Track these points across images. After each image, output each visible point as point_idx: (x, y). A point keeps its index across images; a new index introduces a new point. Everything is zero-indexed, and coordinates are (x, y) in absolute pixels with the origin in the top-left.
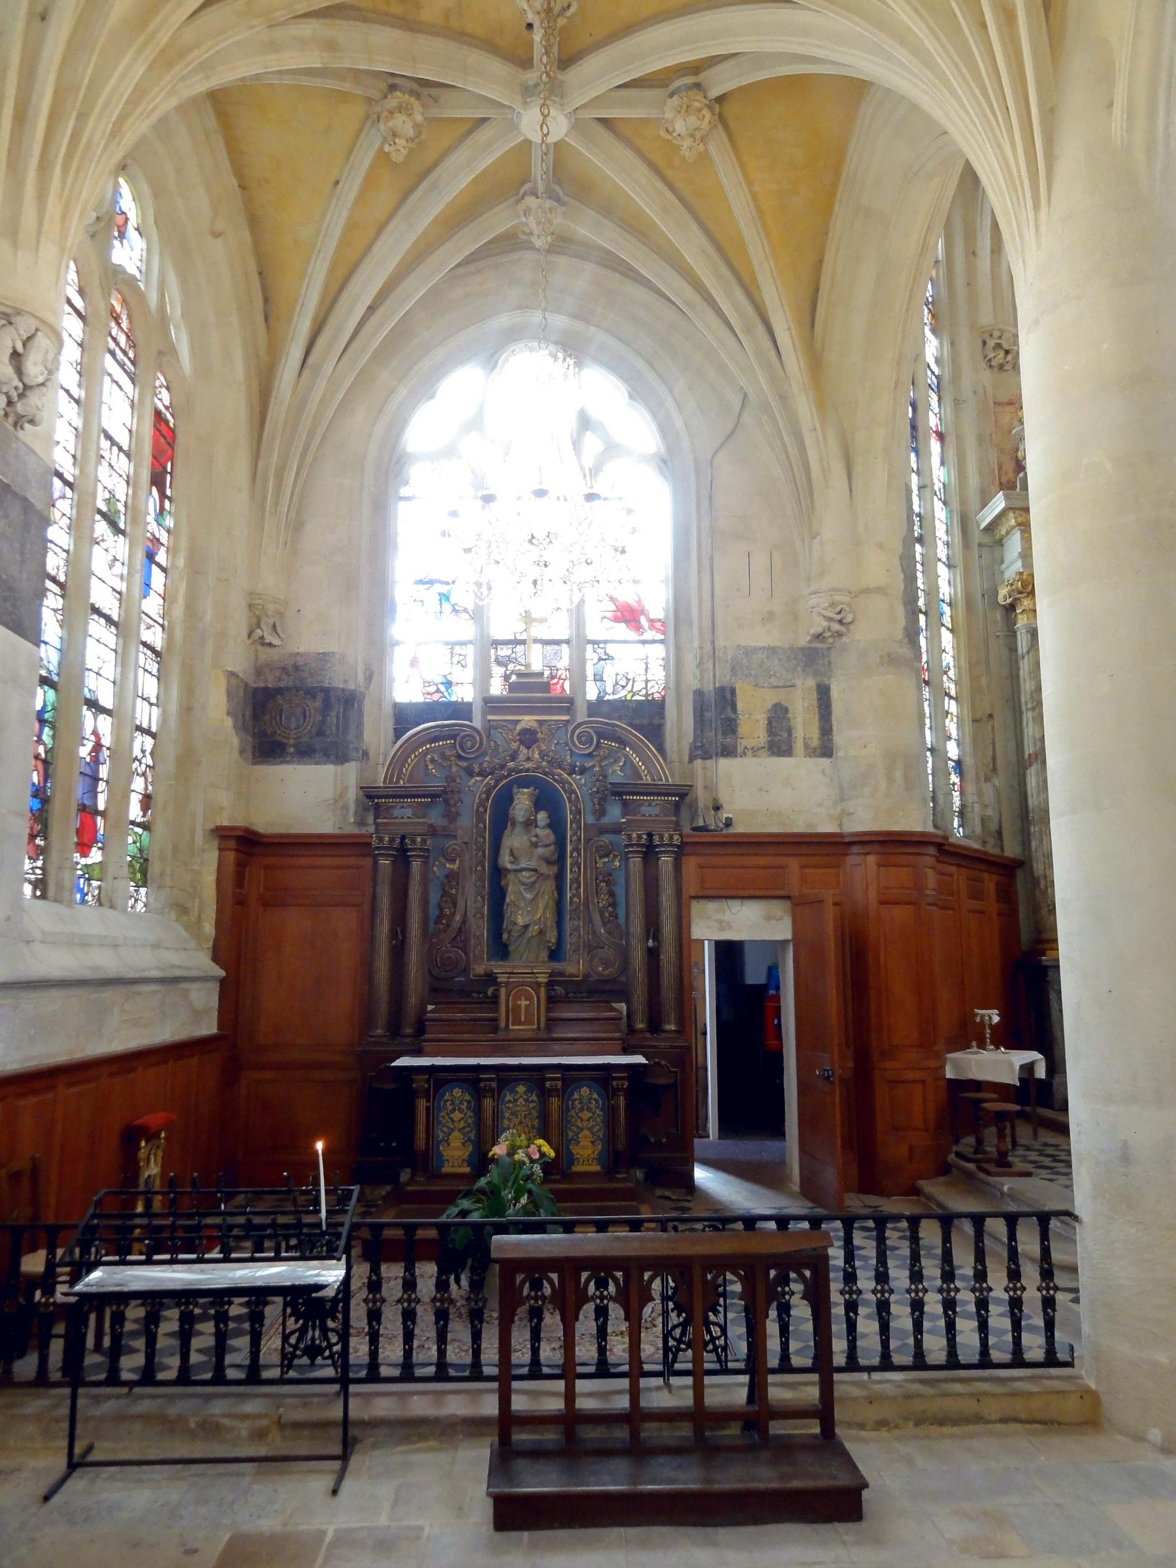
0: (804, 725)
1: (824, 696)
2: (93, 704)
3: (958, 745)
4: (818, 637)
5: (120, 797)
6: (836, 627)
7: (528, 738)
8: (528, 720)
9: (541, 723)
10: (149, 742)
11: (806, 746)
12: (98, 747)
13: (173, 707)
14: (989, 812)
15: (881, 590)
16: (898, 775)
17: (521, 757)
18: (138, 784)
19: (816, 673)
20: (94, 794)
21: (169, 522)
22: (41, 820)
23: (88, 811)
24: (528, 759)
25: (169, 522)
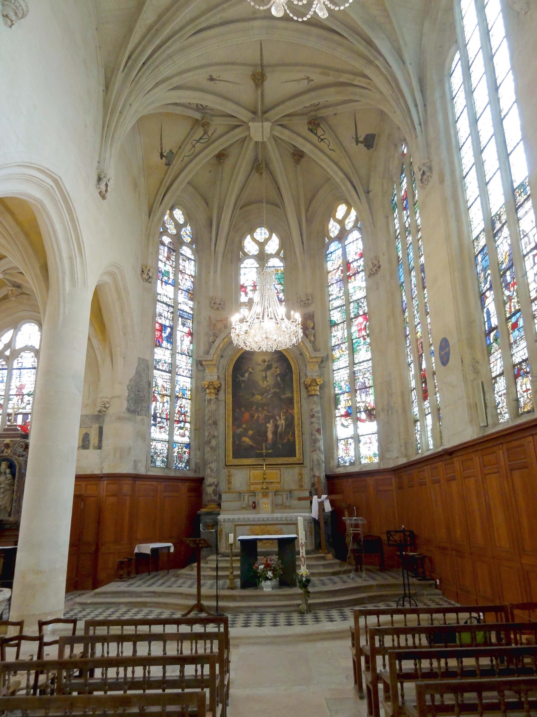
0: (94, 440)
1: (101, 430)
3: (189, 438)
4: (100, 411)
6: (103, 409)
7: (7, 446)
8: (7, 441)
9: (11, 441)
11: (93, 446)
14: (198, 461)
15: (118, 397)
16: (118, 455)
17: (5, 452)
19: (99, 423)
24: (6, 453)
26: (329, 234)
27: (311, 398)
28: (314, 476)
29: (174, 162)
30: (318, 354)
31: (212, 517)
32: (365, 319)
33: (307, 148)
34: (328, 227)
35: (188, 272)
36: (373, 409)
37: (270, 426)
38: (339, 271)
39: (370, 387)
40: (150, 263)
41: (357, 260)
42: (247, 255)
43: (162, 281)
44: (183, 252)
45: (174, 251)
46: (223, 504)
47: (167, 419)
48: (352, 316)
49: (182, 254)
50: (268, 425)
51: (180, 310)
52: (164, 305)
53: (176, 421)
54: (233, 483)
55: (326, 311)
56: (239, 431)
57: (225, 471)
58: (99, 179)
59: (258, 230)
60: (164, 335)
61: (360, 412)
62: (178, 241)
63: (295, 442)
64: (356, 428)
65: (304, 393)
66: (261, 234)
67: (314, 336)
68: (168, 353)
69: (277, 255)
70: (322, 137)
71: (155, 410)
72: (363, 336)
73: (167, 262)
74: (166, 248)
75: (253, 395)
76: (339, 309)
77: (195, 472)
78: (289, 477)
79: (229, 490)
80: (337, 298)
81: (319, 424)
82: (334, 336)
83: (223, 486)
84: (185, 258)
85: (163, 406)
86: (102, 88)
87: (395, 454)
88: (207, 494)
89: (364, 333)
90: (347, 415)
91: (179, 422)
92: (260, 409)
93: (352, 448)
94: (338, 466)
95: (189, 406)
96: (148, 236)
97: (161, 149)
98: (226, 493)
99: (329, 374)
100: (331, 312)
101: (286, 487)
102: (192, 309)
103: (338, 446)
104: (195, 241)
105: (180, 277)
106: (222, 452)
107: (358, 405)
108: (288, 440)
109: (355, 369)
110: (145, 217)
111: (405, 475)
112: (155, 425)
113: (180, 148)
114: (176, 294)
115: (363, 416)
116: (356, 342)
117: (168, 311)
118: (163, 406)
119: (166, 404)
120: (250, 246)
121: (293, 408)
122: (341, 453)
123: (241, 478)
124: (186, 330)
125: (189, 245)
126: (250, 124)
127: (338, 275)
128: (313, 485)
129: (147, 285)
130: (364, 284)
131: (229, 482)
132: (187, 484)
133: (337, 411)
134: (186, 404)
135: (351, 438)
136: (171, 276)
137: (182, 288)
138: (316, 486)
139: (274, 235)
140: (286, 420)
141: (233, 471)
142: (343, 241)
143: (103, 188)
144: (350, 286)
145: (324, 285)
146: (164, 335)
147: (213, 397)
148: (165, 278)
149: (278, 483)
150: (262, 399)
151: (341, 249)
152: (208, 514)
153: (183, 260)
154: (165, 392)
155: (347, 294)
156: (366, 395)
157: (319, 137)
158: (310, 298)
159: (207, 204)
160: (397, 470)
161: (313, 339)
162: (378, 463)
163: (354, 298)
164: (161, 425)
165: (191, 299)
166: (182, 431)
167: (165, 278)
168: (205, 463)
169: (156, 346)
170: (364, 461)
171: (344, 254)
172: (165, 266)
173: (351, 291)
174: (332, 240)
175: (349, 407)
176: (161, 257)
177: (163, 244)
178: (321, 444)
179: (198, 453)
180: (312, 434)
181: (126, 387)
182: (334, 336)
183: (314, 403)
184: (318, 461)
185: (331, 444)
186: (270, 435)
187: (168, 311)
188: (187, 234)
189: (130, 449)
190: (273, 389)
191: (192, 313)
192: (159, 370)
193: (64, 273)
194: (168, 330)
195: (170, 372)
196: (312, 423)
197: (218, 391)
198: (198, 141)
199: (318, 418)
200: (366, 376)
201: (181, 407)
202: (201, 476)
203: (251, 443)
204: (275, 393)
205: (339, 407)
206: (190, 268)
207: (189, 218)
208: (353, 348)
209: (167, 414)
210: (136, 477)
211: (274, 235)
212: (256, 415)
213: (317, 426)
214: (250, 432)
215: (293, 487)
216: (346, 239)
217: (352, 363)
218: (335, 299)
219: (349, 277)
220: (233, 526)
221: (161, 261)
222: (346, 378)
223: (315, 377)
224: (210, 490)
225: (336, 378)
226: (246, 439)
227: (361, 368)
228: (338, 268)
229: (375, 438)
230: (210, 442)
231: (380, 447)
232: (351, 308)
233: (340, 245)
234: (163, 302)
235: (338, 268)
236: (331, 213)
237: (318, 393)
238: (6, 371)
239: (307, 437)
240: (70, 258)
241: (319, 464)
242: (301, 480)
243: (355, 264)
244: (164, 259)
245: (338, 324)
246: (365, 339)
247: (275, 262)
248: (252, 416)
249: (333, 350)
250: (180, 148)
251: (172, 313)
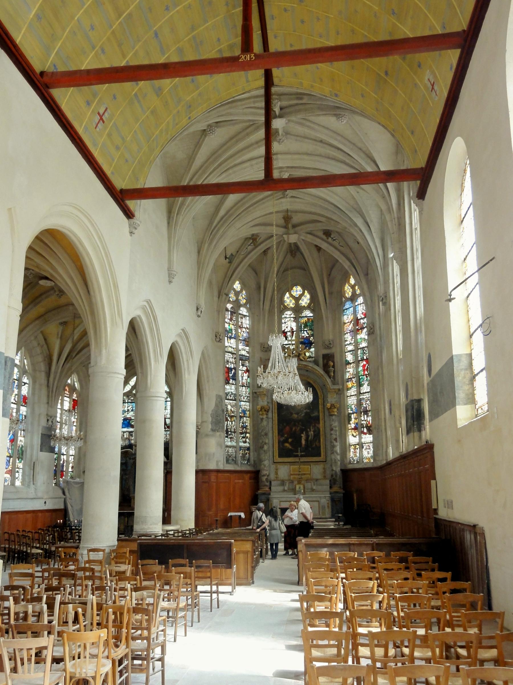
2: (63, 454)
3: (249, 444)
5: (67, 468)
10: (73, 457)
12: (64, 461)
13: (77, 450)
14: (256, 459)
18: (71, 465)
20: (63, 469)
21: (76, 417)
22: (55, 474)
23: (62, 471)
25: (76, 417)
26: (345, 294)
27: (331, 417)
28: (332, 470)
29: (234, 261)
30: (336, 387)
31: (266, 496)
32: (367, 362)
33: (324, 246)
34: (344, 289)
35: (245, 326)
36: (371, 426)
37: (303, 436)
38: (352, 324)
39: (369, 411)
40: (221, 330)
41: (363, 318)
42: (286, 308)
43: (228, 337)
44: (241, 312)
45: (235, 313)
46: (272, 488)
48: (359, 358)
49: (240, 314)
50: (302, 435)
51: (241, 355)
52: (230, 354)
53: (240, 433)
54: (279, 473)
55: (343, 353)
56: (282, 439)
57: (273, 467)
58: (197, 309)
59: (294, 288)
60: (231, 375)
61: (363, 427)
62: (237, 305)
63: (320, 447)
64: (360, 438)
65: (327, 413)
66: (297, 291)
67: (334, 373)
68: (233, 387)
69: (309, 307)
70: (334, 238)
71: (227, 427)
72: (366, 375)
73: (231, 323)
74: (229, 312)
75: (292, 414)
76: (351, 352)
77: (254, 466)
78: (317, 470)
79: (277, 479)
80: (350, 344)
81: (336, 435)
82: (348, 372)
83: (272, 476)
84: (242, 316)
85: (232, 423)
86: (197, 254)
87: (381, 458)
88: (262, 481)
89: (366, 373)
90: (355, 429)
91: (241, 433)
92: (297, 424)
93: (358, 451)
94: (350, 463)
95: (248, 422)
96: (219, 312)
97: (226, 254)
98: (274, 480)
99: (344, 399)
100: (346, 354)
101: (315, 477)
102: (248, 352)
103: (350, 450)
104: (249, 300)
105: (240, 331)
106: (271, 453)
107: (362, 422)
108: (316, 445)
109: (361, 397)
110: (216, 299)
111: (381, 471)
112: (227, 437)
113: (238, 252)
114: (237, 345)
115: (365, 430)
116: (362, 378)
118: (232, 423)
119: (233, 423)
120: (289, 301)
121: (319, 423)
122: (352, 454)
123: (284, 471)
124: (245, 368)
125: (245, 305)
126: (284, 236)
127: (350, 327)
128: (332, 476)
129: (219, 344)
130: (366, 337)
131: (277, 473)
132: (249, 475)
133: (349, 425)
134: (247, 421)
135: (358, 444)
136: (234, 332)
137: (241, 339)
138: (334, 477)
139: (306, 292)
140: (314, 432)
141: (279, 466)
142: (354, 302)
143: (199, 313)
144: (359, 337)
145: (341, 333)
146: (231, 375)
147: (265, 416)
148: (230, 334)
149: (310, 474)
150: (298, 417)
151: (352, 308)
152: (264, 494)
153: (242, 318)
155: (356, 344)
156: (367, 416)
157: (332, 238)
158: (331, 342)
159: (256, 273)
160: (381, 468)
161: (332, 374)
162: (373, 463)
163: (361, 346)
164: (231, 436)
165: (247, 346)
166: (244, 439)
167: (230, 334)
168: (260, 461)
170: (365, 461)
171: (355, 312)
172: (229, 325)
173: (359, 340)
174: (348, 299)
175: (357, 423)
176: (226, 320)
177: (227, 310)
178: (338, 449)
179: (256, 453)
180: (331, 442)
181: (210, 416)
182: (348, 372)
183: (333, 420)
184: (335, 460)
185: (345, 448)
186: (303, 442)
188: (243, 298)
189: (214, 454)
190: (305, 409)
191: (248, 355)
192: (228, 399)
193: (185, 369)
194: (233, 371)
195: (235, 400)
196: (331, 434)
197: (268, 412)
198: (249, 245)
199: (336, 431)
200: (367, 403)
202: (258, 469)
203: (290, 447)
204: (306, 413)
205: (351, 422)
206: (246, 322)
207: (244, 285)
208: (360, 382)
210: (218, 471)
211: (306, 292)
212: (294, 429)
213: (334, 437)
214: (290, 440)
215: (319, 477)
216: (356, 301)
217: (359, 393)
218: (349, 344)
219: (358, 330)
220: (278, 503)
221: (227, 323)
222: (355, 403)
223: (333, 403)
224: (264, 479)
225: (349, 402)
226: (287, 445)
227: (364, 397)
228: (351, 322)
229: (371, 445)
230: (263, 447)
231: (374, 452)
232: (359, 353)
233: (352, 305)
234: (229, 352)
235: (351, 322)
236: (346, 279)
237: (336, 413)
238: (134, 404)
239: (328, 444)
240: (187, 360)
241: (336, 462)
242: (325, 472)
243: (362, 321)
244: (229, 321)
245: (351, 364)
246: (367, 377)
247: (308, 313)
248: (291, 429)
249: (348, 382)
250: (238, 252)
251: (235, 358)
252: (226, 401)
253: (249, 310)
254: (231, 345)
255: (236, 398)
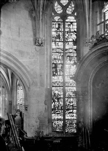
47: (61, 109)
68: (61, 77)
112: (55, 113)
117: (60, 56)
154: (60, 97)
169: (54, 75)
187: (60, 56)
201: (70, 102)
209: (61, 107)
252: (53, 88)
253: (76, 18)
254: (59, 47)
255: (64, 85)
